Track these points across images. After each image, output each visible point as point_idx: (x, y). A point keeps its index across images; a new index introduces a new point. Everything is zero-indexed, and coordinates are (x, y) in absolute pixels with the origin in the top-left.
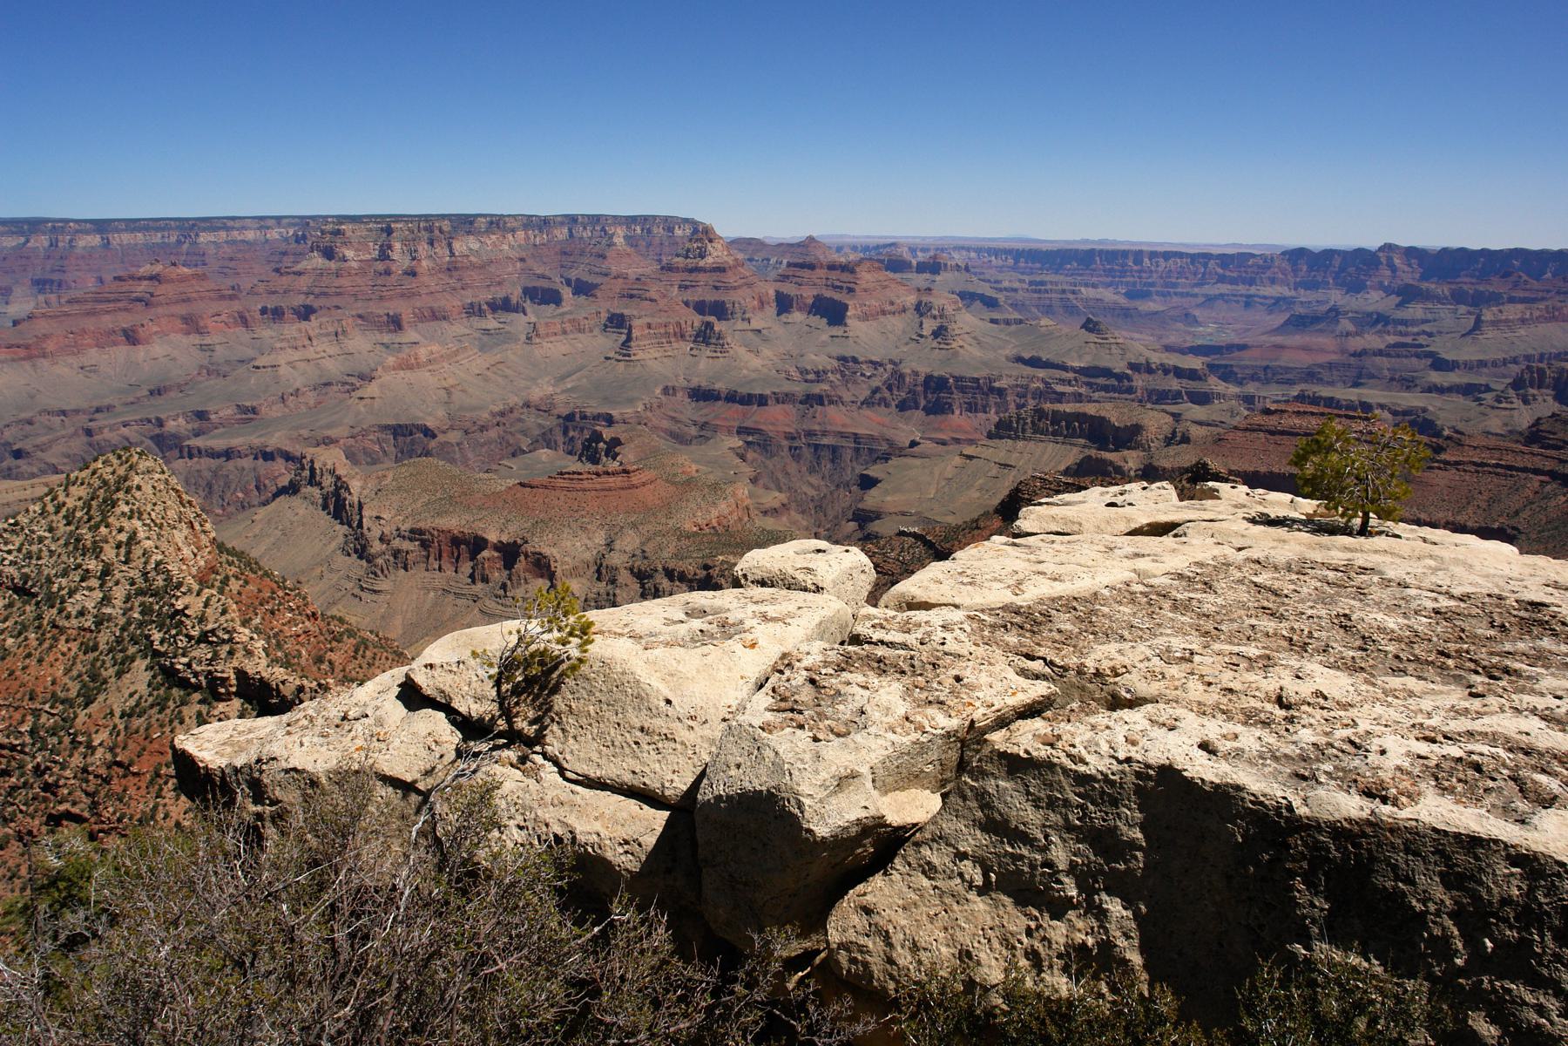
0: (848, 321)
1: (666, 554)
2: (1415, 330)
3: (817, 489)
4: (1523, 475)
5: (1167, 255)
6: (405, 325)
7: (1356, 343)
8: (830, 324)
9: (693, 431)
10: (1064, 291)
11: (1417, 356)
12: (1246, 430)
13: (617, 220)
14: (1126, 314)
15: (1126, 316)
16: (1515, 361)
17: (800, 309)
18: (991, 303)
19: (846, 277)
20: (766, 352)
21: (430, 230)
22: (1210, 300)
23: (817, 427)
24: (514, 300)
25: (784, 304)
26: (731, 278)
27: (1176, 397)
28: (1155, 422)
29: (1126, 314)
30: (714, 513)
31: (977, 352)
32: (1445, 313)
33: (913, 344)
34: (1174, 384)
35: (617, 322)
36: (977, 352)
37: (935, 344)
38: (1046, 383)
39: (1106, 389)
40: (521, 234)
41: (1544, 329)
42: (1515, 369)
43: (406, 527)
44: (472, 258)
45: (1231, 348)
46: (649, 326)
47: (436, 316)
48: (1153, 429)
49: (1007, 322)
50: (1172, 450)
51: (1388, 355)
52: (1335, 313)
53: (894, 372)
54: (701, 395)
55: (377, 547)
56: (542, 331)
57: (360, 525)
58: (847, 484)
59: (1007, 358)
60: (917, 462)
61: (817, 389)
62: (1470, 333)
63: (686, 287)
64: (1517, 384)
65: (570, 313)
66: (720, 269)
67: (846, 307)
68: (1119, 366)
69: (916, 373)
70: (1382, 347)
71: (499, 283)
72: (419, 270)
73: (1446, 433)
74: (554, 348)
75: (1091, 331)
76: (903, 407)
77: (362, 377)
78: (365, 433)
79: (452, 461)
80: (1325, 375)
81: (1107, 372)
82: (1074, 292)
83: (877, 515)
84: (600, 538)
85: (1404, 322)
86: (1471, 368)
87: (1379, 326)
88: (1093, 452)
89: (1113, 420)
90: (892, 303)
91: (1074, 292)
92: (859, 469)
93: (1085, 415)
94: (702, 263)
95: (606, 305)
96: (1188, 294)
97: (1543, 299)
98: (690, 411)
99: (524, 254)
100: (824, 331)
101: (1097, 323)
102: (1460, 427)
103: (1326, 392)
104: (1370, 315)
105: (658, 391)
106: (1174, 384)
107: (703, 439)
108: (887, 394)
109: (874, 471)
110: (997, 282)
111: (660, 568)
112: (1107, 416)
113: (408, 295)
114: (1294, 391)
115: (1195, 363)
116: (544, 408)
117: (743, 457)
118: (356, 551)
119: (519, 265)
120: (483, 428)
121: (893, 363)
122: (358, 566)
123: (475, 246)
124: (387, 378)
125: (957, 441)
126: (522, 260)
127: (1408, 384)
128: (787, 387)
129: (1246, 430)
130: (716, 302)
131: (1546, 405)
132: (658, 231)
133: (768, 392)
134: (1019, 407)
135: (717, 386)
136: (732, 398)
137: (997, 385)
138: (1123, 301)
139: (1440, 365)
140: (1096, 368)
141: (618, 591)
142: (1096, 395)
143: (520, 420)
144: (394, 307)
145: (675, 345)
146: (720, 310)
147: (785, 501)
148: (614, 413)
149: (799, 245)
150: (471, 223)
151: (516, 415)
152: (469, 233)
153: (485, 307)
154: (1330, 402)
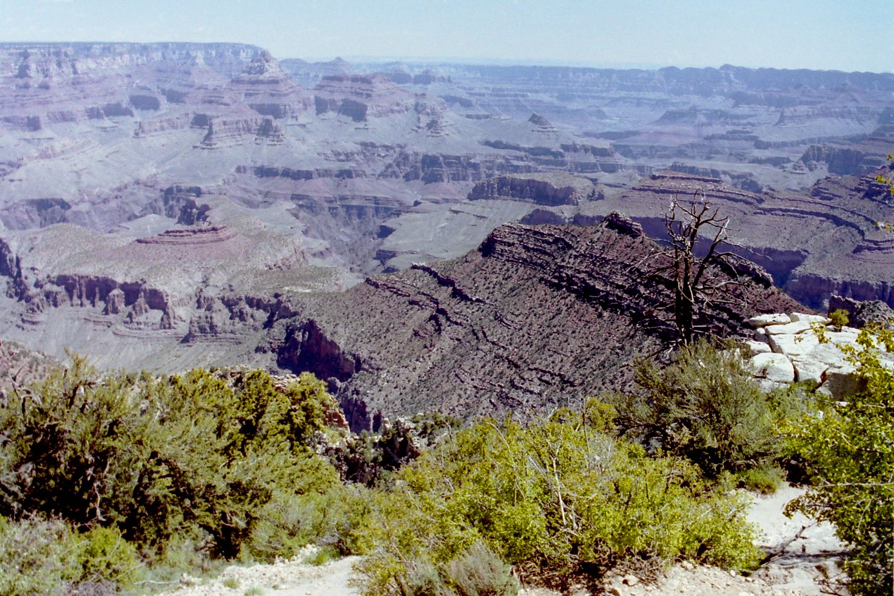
0: (368, 118)
1: (247, 287)
2: (745, 121)
3: (350, 236)
4: (810, 217)
5: (585, 71)
6: (43, 126)
7: (708, 131)
8: (355, 120)
9: (260, 198)
10: (516, 95)
11: (746, 139)
12: (640, 190)
13: (198, 46)
14: (559, 111)
15: (559, 112)
16: (804, 142)
17: (333, 110)
18: (466, 104)
19: (365, 86)
20: (311, 140)
21: (57, 54)
22: (614, 101)
23: (348, 193)
24: (124, 106)
25: (321, 106)
26: (282, 88)
27: (592, 167)
28: (580, 184)
29: (559, 111)
30: (280, 257)
31: (457, 137)
32: (761, 110)
33: (414, 133)
34: (591, 159)
35: (201, 121)
36: (457, 137)
37: (429, 133)
38: (507, 160)
39: (547, 163)
40: (126, 57)
41: (821, 121)
42: (804, 148)
43: (55, 274)
44: (91, 75)
45: (629, 134)
46: (225, 123)
47: (65, 118)
48: (579, 190)
49: (478, 117)
50: (594, 204)
51: (728, 139)
52: (694, 111)
53: (401, 154)
54: (264, 172)
55: (33, 291)
56: (146, 127)
57: (19, 274)
58: (371, 233)
59: (479, 142)
60: (418, 216)
61: (347, 166)
62: (777, 124)
63: (251, 95)
64: (805, 159)
65: (166, 114)
66: (275, 82)
67: (365, 107)
68: (556, 147)
69: (416, 154)
70: (724, 133)
71: (112, 94)
72: (51, 84)
73: (764, 190)
74: (156, 140)
75: (536, 122)
76: (407, 177)
77: (11, 164)
78: (15, 206)
79: (84, 225)
80: (689, 152)
81: (547, 152)
82: (523, 96)
83: (393, 255)
84: (199, 277)
85: (738, 117)
86: (778, 147)
87: (722, 120)
88: (540, 207)
89: (553, 184)
90: (398, 105)
91: (523, 96)
92: (379, 222)
93: (534, 181)
94: (261, 77)
95: (193, 108)
96: (598, 98)
97: (820, 102)
98: (255, 183)
99: (129, 72)
100: (351, 125)
101: (540, 118)
102: (773, 186)
103: (689, 163)
104: (716, 112)
105: (233, 170)
106: (591, 159)
107: (267, 203)
108: (396, 169)
109: (390, 223)
110: (470, 89)
111: (244, 298)
112: (549, 181)
113: (44, 103)
114: (670, 163)
115: (605, 144)
116: (149, 185)
117: (296, 216)
118: (17, 294)
119: (126, 80)
120: (105, 201)
121: (401, 147)
122: (22, 307)
123: (93, 65)
124: (31, 165)
125: (447, 201)
126: (129, 76)
127: (740, 157)
128: (326, 165)
129: (640, 190)
130: (272, 105)
131: (822, 171)
132: (229, 54)
133: (312, 169)
134: (489, 176)
135: (275, 166)
136: (286, 173)
137: (472, 161)
138: (557, 102)
139: (759, 145)
140: (540, 148)
141: (214, 315)
142: (540, 168)
143: (132, 194)
144: (33, 111)
145: (244, 137)
146: (276, 111)
147: (328, 246)
148: (202, 186)
149: (330, 64)
150: (89, 49)
151: (129, 190)
152: (87, 56)
153: (102, 111)
154: (692, 170)
